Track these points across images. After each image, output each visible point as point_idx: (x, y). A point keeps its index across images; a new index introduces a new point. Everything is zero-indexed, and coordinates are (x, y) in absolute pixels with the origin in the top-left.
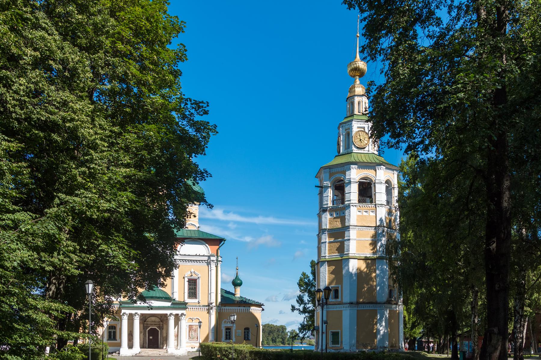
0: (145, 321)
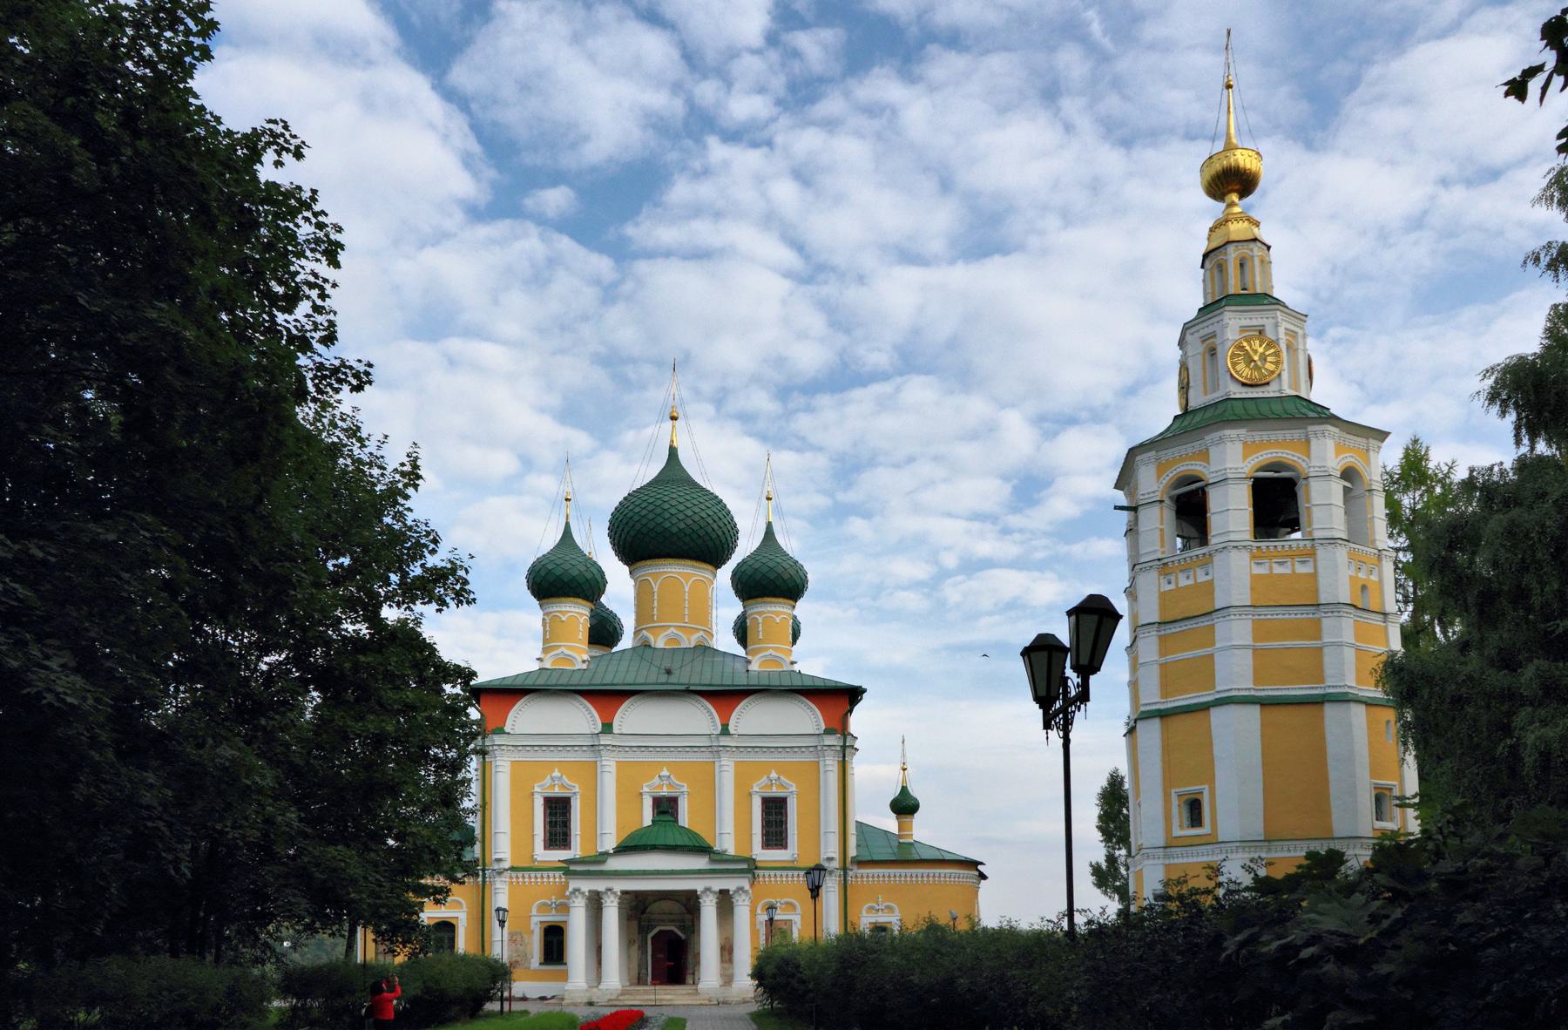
0: (643, 912)
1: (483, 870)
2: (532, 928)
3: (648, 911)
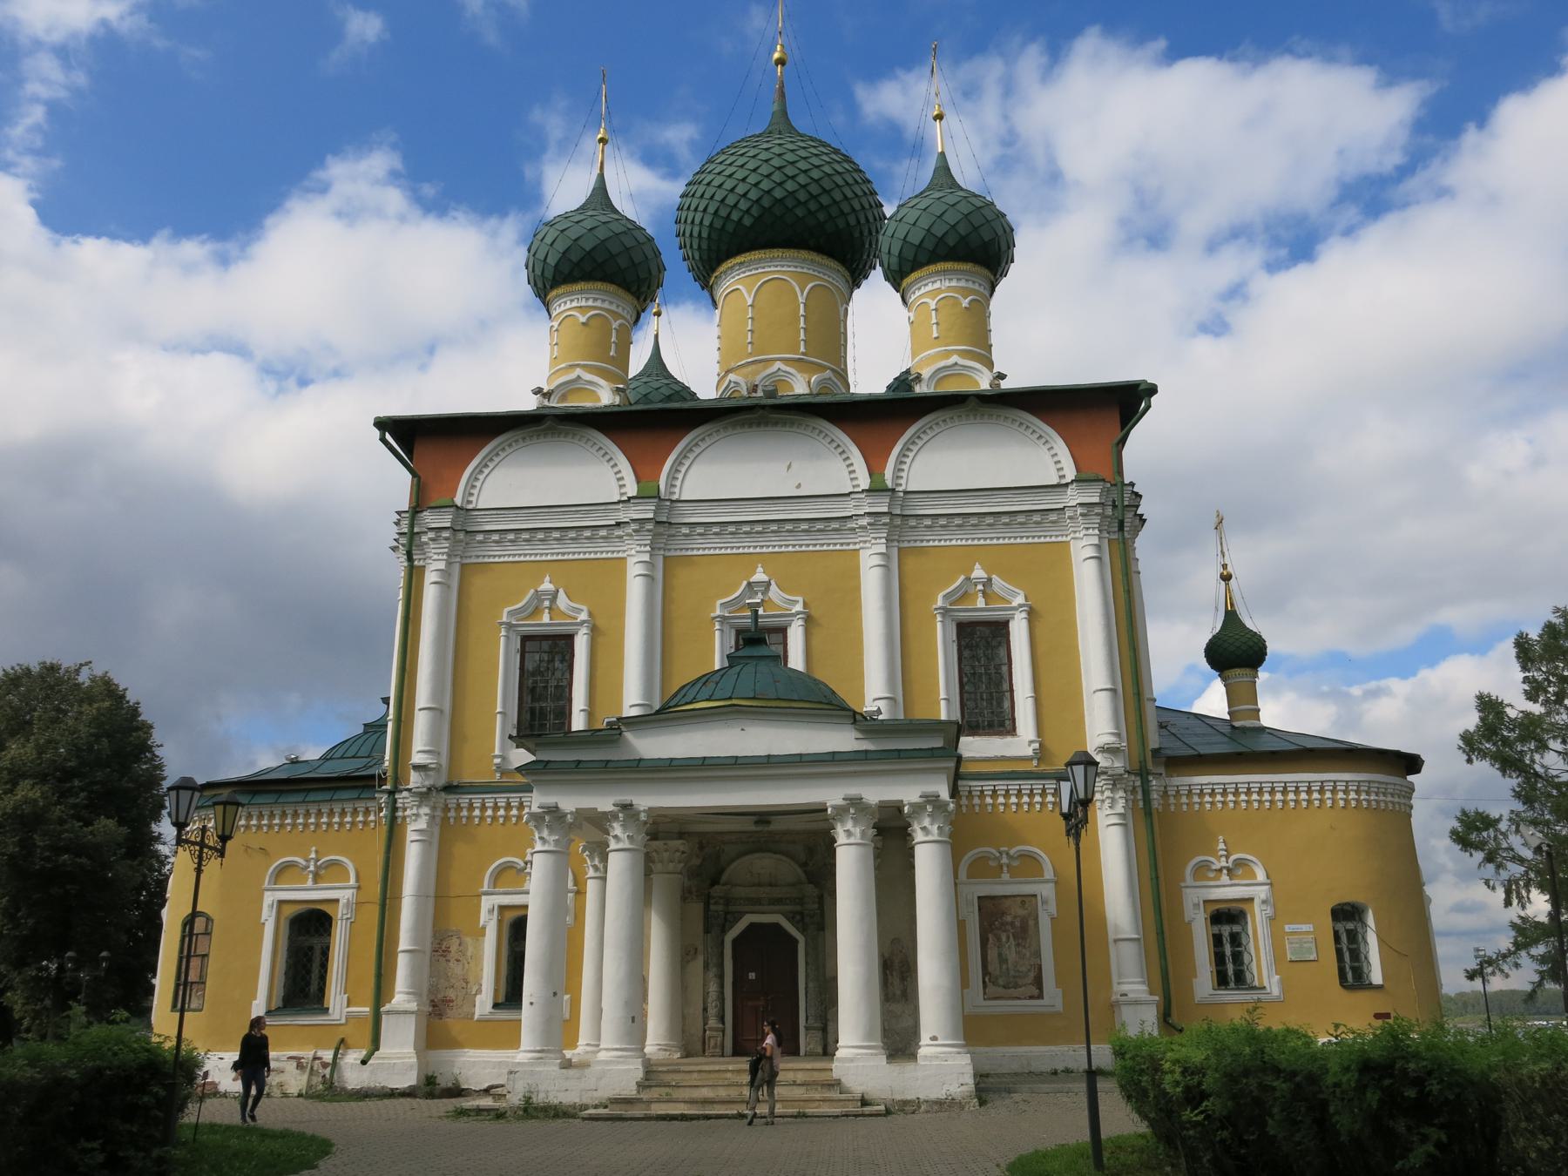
0: (715, 882)
1: (391, 793)
2: (482, 923)
3: (724, 878)
